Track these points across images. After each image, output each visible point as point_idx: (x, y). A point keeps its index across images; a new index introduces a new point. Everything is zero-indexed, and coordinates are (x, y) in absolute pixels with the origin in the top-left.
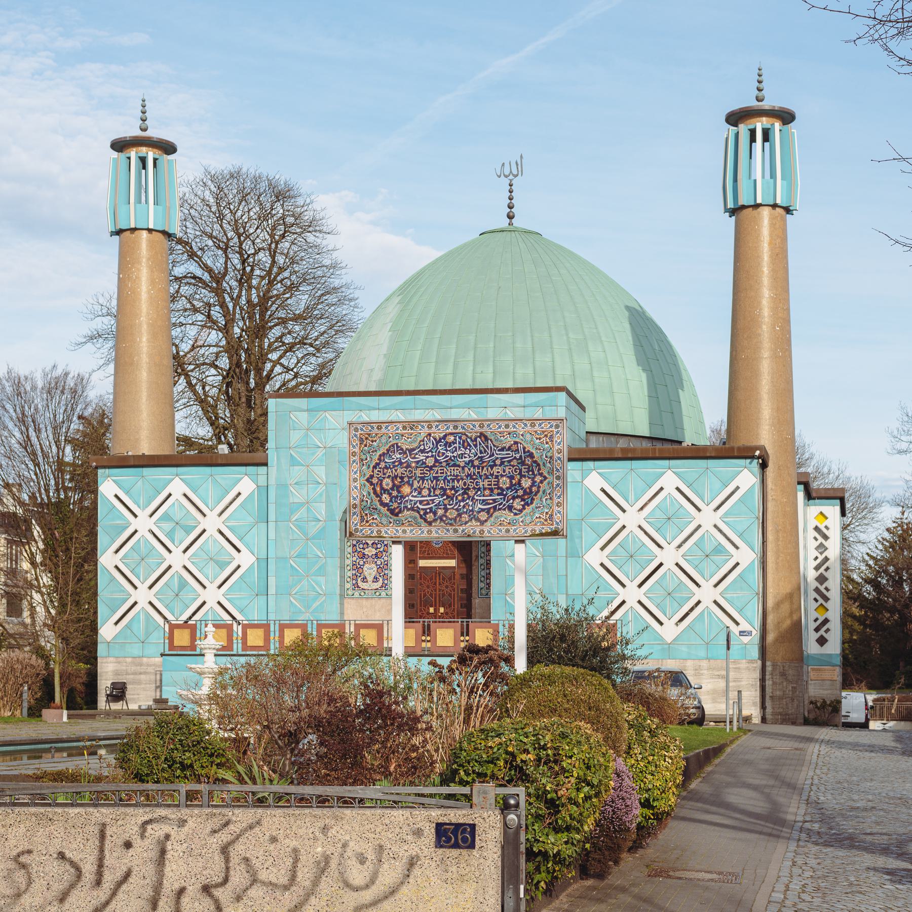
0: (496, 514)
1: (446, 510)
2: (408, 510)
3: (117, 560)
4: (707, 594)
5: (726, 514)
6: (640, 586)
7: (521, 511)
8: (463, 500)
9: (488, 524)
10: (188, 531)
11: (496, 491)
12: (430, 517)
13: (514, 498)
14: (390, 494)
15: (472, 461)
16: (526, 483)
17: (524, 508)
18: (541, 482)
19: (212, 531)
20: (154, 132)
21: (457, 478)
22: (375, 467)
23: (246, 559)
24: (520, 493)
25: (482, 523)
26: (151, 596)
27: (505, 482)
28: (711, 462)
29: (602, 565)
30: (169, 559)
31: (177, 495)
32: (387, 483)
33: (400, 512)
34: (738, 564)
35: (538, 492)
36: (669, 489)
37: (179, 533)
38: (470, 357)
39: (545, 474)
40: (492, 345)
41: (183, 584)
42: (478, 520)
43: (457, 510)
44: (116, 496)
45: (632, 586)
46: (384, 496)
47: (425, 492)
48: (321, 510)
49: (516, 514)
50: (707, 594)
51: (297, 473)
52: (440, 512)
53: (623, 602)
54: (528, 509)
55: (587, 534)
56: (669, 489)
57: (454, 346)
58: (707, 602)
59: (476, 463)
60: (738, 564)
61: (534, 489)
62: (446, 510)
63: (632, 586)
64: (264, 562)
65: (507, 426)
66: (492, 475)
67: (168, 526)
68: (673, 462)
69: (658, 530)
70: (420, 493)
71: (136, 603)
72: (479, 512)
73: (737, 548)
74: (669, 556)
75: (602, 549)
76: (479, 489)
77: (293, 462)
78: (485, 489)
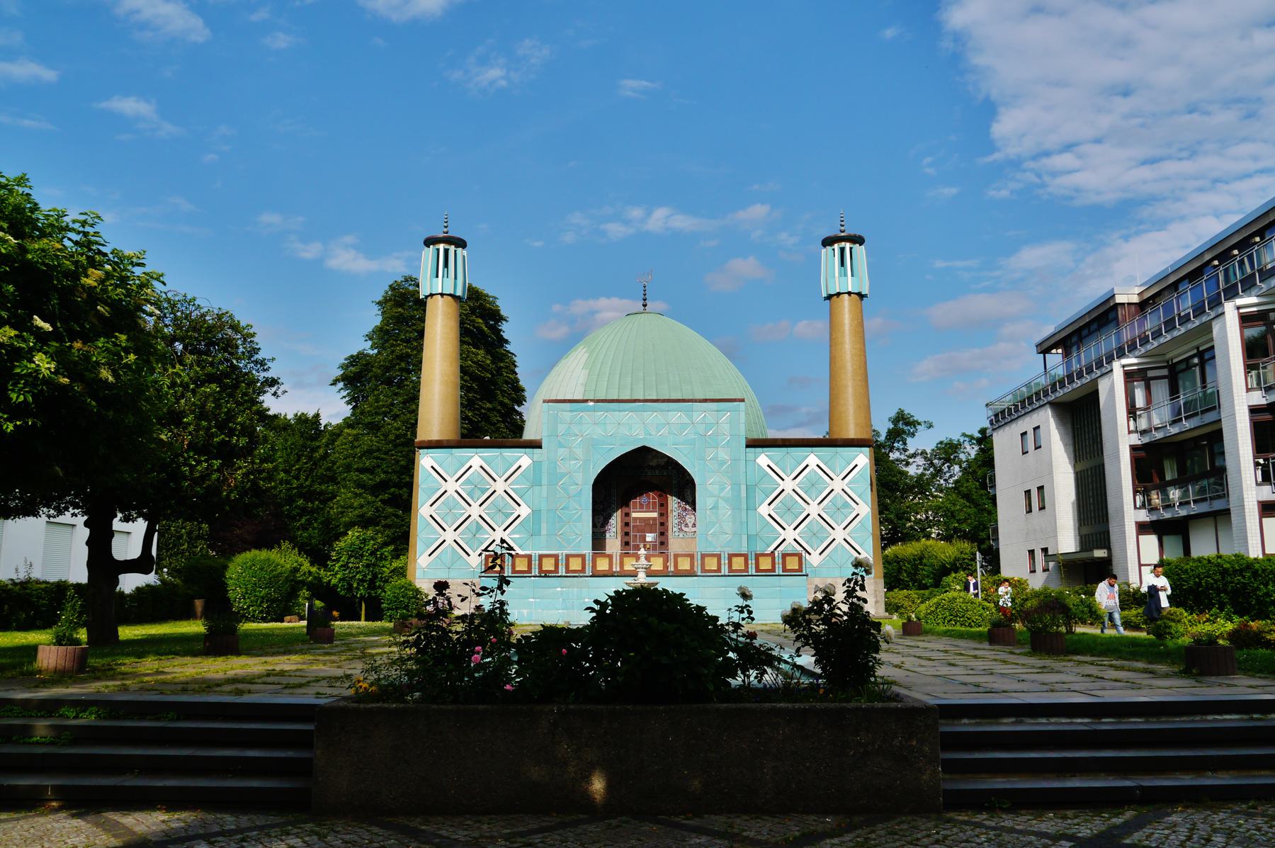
3: (432, 511)
4: (839, 534)
5: (850, 483)
10: (484, 491)
19: (500, 492)
20: (453, 233)
23: (524, 511)
26: (456, 536)
30: (469, 511)
36: (813, 466)
37: (478, 493)
41: (479, 528)
45: (790, 529)
48: (579, 477)
50: (839, 534)
51: (561, 451)
56: (813, 466)
58: (839, 540)
63: (790, 529)
64: (536, 513)
67: (469, 487)
74: (814, 509)
77: (561, 445)
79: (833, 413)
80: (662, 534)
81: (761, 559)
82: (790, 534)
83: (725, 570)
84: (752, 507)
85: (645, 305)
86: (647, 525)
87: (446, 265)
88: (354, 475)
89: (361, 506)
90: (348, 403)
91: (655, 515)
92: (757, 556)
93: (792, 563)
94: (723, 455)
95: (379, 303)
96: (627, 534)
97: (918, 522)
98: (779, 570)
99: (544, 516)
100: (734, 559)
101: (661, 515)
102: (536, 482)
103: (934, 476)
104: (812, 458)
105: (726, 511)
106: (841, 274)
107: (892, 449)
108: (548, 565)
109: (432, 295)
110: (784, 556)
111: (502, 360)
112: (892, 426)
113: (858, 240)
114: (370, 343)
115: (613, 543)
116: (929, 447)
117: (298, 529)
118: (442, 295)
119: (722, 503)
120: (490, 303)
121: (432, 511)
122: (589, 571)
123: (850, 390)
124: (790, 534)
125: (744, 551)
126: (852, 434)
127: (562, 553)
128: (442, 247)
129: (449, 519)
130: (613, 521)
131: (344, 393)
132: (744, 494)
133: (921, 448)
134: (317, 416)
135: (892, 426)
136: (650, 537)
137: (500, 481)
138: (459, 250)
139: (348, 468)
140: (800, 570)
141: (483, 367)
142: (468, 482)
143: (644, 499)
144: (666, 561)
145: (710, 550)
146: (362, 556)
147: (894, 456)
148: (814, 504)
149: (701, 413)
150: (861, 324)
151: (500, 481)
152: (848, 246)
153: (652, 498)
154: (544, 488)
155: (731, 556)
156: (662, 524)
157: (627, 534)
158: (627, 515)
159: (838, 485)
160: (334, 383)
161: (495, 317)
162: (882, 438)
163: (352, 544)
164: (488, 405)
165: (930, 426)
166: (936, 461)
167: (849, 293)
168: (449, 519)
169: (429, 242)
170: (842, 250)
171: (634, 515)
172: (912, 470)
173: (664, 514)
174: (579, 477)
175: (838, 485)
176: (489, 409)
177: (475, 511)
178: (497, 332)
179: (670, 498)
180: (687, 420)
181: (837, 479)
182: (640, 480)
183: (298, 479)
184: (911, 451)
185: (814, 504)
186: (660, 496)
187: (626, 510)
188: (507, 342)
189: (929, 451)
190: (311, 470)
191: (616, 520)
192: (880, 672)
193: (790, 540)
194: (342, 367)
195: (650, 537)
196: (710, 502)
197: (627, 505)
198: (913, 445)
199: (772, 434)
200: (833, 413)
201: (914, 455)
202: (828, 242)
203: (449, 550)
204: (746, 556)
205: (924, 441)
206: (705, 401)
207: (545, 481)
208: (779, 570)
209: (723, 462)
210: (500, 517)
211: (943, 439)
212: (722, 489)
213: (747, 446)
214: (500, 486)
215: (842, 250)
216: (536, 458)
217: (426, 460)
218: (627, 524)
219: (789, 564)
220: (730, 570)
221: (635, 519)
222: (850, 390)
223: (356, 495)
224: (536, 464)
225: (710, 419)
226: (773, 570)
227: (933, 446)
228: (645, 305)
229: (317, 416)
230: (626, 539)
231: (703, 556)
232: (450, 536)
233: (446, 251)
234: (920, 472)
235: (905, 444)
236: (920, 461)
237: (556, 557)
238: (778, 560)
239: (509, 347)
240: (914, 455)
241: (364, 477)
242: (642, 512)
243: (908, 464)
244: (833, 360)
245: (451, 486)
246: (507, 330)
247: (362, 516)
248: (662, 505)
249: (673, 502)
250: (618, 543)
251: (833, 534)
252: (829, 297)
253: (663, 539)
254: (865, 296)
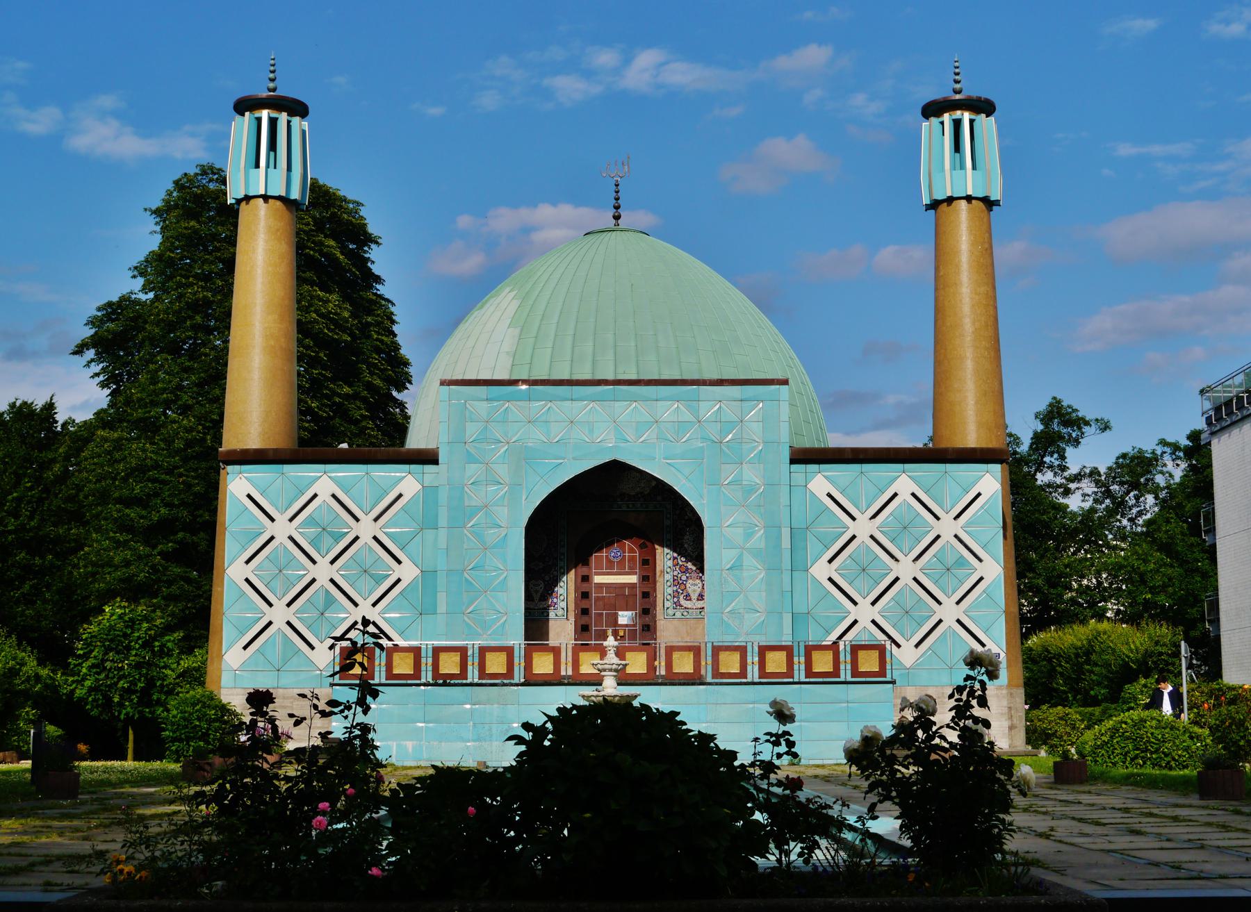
3: (248, 571)
4: (949, 612)
6: (873, 603)
10: (338, 537)
19: (366, 538)
20: (285, 90)
23: (408, 572)
28: (950, 467)
29: (830, 579)
31: (324, 496)
34: (981, 579)
37: (328, 540)
38: (610, 356)
40: (633, 344)
44: (249, 496)
45: (864, 603)
50: (949, 612)
51: (473, 470)
53: (855, 622)
55: (812, 545)
57: (591, 344)
60: (981, 579)
63: (864, 603)
64: (428, 575)
67: (312, 531)
68: (907, 466)
71: (270, 623)
73: (980, 560)
74: (906, 569)
75: (830, 561)
77: (471, 459)
79: (940, 407)
80: (646, 612)
81: (816, 655)
82: (865, 613)
83: (753, 673)
84: (799, 566)
85: (617, 218)
86: (621, 598)
87: (273, 146)
88: (114, 510)
89: (127, 564)
90: (103, 385)
91: (633, 579)
92: (809, 650)
93: (869, 662)
94: (751, 475)
95: (157, 212)
96: (585, 612)
97: (1083, 591)
98: (845, 673)
99: (441, 580)
100: (770, 656)
101: (644, 578)
102: (428, 523)
103: (1111, 513)
104: (904, 481)
106: (953, 166)
107: (1040, 466)
108: (449, 665)
109: (248, 198)
110: (855, 649)
111: (370, 312)
112: (1040, 427)
113: (983, 107)
114: (140, 281)
115: (562, 630)
116: (1103, 465)
117: (18, 602)
118: (266, 198)
119: (749, 561)
120: (349, 213)
121: (248, 571)
122: (519, 676)
123: (969, 365)
124: (865, 613)
125: (786, 640)
126: (972, 438)
127: (474, 644)
128: (265, 114)
129: (277, 584)
130: (561, 589)
131: (96, 368)
132: (786, 543)
133: (1090, 465)
134: (50, 407)
135: (1040, 427)
136: (624, 617)
137: (367, 520)
138: (296, 120)
139: (103, 497)
140: (882, 672)
141: (339, 325)
142: (311, 521)
143: (613, 552)
144: (652, 658)
145: (728, 640)
146: (128, 648)
147: (1044, 478)
148: (906, 561)
149: (713, 402)
150: (989, 251)
151: (367, 520)
152: (966, 116)
153: (628, 549)
154: (443, 533)
155: (763, 650)
156: (646, 595)
157: (585, 612)
158: (586, 579)
159: (947, 527)
160: (79, 350)
161: (357, 236)
162: (1024, 448)
163: (111, 628)
164: (346, 389)
165: (1105, 427)
166: (1115, 488)
167: (969, 199)
168: (277, 584)
169: (244, 106)
170: (957, 124)
171: (598, 579)
172: (1075, 503)
173: (649, 578)
174: (502, 514)
175: (947, 527)
176: (347, 397)
177: (323, 571)
178: (362, 263)
179: (659, 550)
180: (690, 418)
181: (947, 518)
182: (607, 520)
183: (16, 517)
184: (1074, 469)
185: (906, 561)
186: (641, 547)
187: (583, 570)
188: (378, 279)
189: (1103, 470)
190: (41, 501)
191: (566, 588)
192: (1013, 844)
193: (864, 622)
194: (92, 322)
195: (624, 617)
196: (729, 556)
197: (586, 563)
198: (1076, 459)
199: (836, 440)
200: (940, 407)
201: (1077, 478)
202: (933, 110)
203: (279, 639)
204: (789, 650)
205: (1092, 453)
206: (720, 382)
207: (443, 522)
208: (845, 673)
209: (751, 489)
210: (366, 582)
211: (1127, 449)
212: (748, 536)
213: (792, 461)
214: (366, 529)
215: (957, 124)
216: (428, 480)
217: (238, 485)
218: (585, 595)
219: (866, 663)
220: (763, 673)
221: (600, 586)
222: (969, 365)
223: (118, 544)
224: (429, 492)
225: (730, 414)
226: (836, 673)
227: (1110, 461)
228: (617, 218)
229: (50, 407)
230: (584, 620)
231: (717, 650)
232: (279, 614)
233: (273, 123)
234: (1087, 505)
235: (1063, 457)
236: (1088, 486)
237: (463, 651)
238: (845, 657)
239: (382, 290)
240: (1077, 478)
241: (132, 513)
242: (612, 574)
243: (1067, 492)
244: (940, 312)
245: (282, 529)
246: (379, 259)
247: (128, 580)
248: (645, 562)
249: (665, 558)
250: (570, 627)
251: (940, 612)
252: (935, 205)
253: (647, 619)
254: (997, 203)
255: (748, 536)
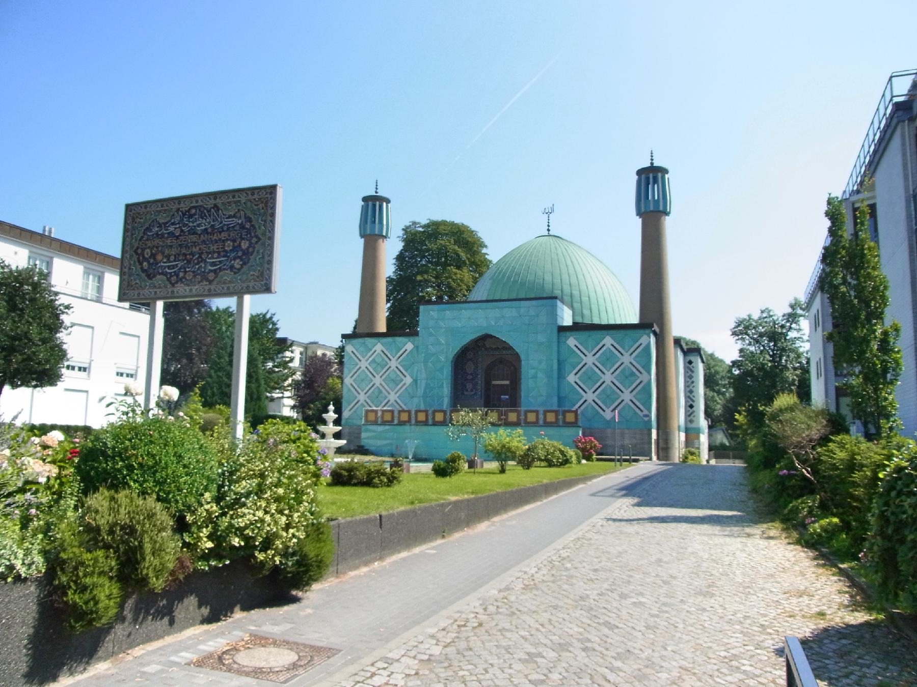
0: (221, 273)
1: (185, 272)
2: (160, 274)
5: (637, 357)
7: (239, 270)
8: (198, 264)
9: (215, 283)
11: (222, 254)
12: (174, 279)
13: (235, 259)
14: (148, 262)
15: (206, 229)
16: (245, 245)
17: (242, 267)
18: (257, 243)
21: (194, 244)
22: (140, 240)
24: (240, 254)
25: (210, 282)
27: (229, 245)
32: (147, 254)
33: (154, 276)
35: (253, 252)
37: (379, 368)
39: (260, 236)
42: (207, 280)
43: (194, 272)
46: (145, 264)
47: (172, 258)
49: (235, 273)
51: (431, 339)
52: (181, 274)
54: (245, 268)
55: (568, 367)
59: (209, 230)
61: (251, 250)
62: (185, 272)
63: (590, 392)
65: (234, 197)
66: (220, 239)
69: (603, 365)
70: (168, 259)
72: (208, 273)
76: (210, 253)
78: (214, 252)
84: (561, 376)
85: (549, 230)
91: (507, 382)
92: (565, 412)
100: (549, 415)
105: (542, 378)
108: (404, 417)
122: (430, 422)
125: (555, 408)
132: (555, 367)
148: (608, 374)
212: (540, 363)
251: (623, 396)
255: (540, 363)
